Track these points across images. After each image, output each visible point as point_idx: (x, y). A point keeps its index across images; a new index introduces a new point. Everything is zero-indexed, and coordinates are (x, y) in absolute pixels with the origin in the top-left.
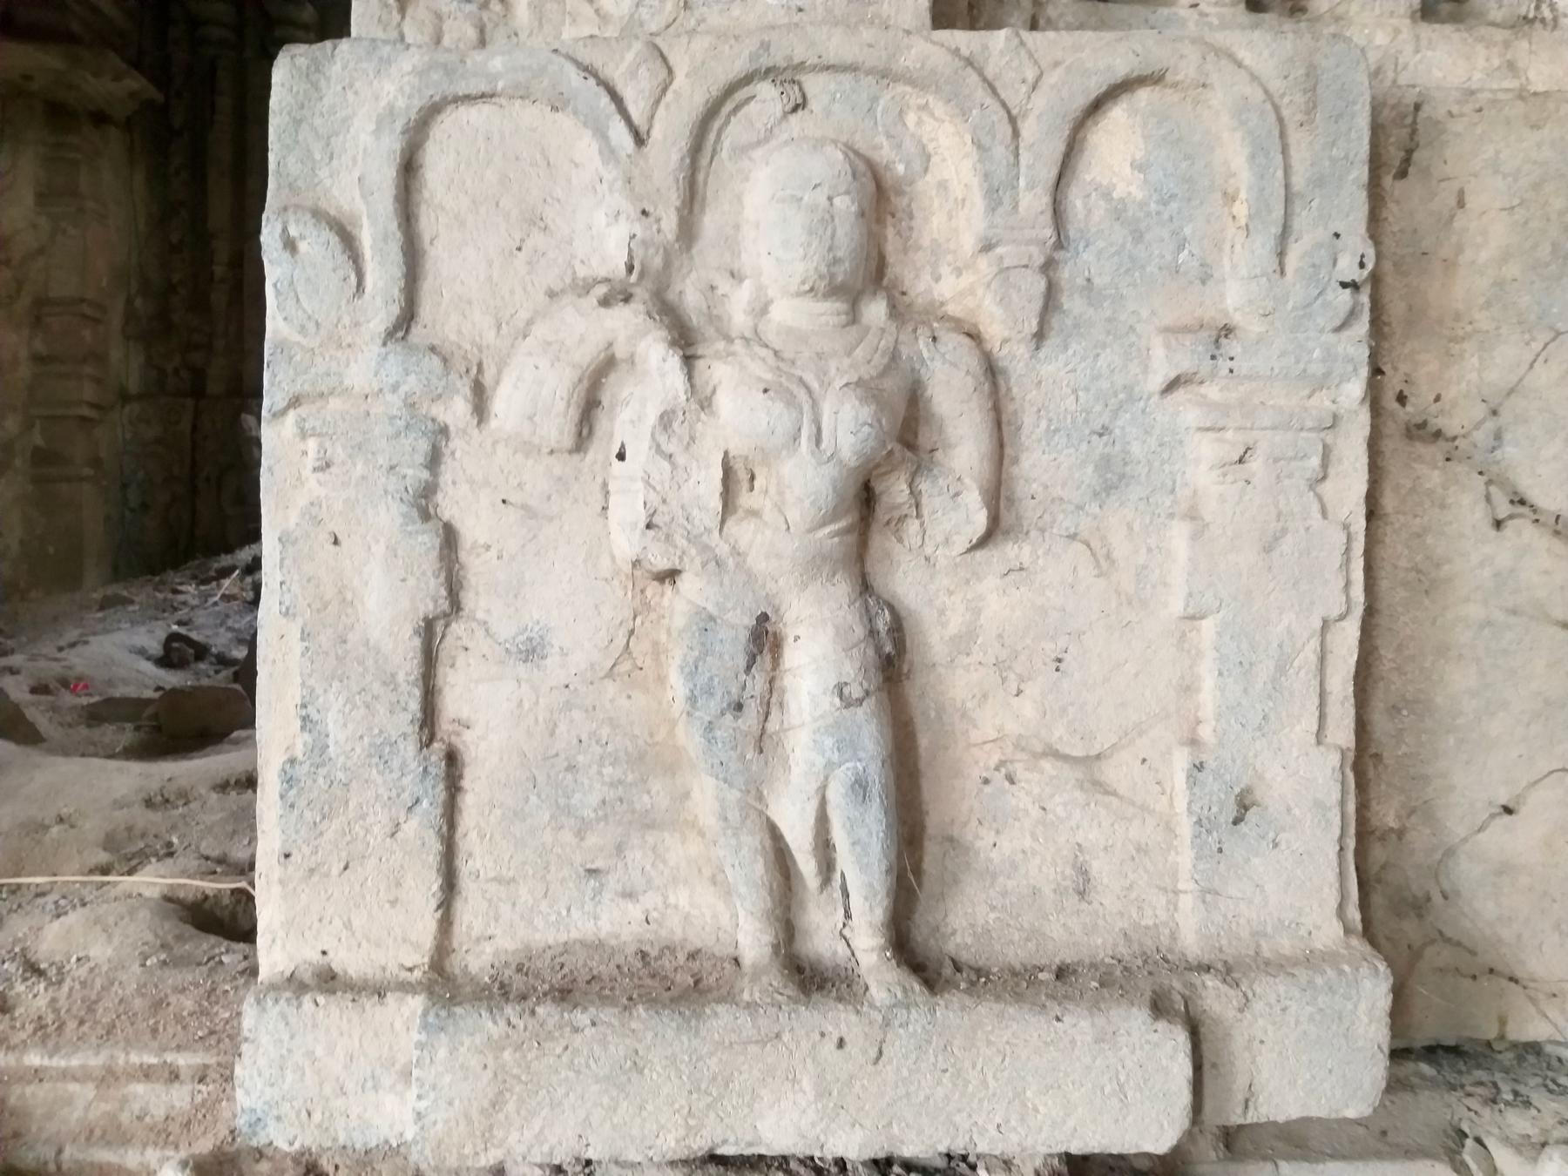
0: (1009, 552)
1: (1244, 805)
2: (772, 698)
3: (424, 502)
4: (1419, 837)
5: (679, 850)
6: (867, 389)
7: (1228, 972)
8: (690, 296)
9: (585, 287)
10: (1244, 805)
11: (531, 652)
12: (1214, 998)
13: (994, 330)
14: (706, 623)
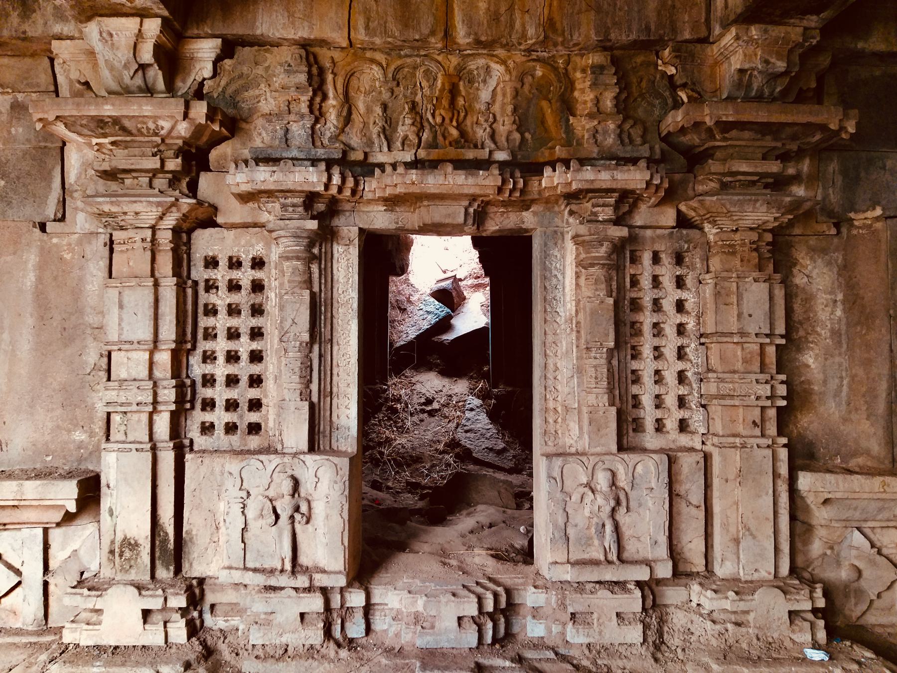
0: (629, 514)
1: (656, 543)
2: (604, 532)
3: (565, 510)
4: (679, 545)
5: (593, 548)
6: (614, 499)
7: (654, 561)
8: (593, 486)
9: (581, 485)
10: (656, 543)
11: (576, 526)
12: (653, 564)
13: (626, 489)
14: (597, 524)
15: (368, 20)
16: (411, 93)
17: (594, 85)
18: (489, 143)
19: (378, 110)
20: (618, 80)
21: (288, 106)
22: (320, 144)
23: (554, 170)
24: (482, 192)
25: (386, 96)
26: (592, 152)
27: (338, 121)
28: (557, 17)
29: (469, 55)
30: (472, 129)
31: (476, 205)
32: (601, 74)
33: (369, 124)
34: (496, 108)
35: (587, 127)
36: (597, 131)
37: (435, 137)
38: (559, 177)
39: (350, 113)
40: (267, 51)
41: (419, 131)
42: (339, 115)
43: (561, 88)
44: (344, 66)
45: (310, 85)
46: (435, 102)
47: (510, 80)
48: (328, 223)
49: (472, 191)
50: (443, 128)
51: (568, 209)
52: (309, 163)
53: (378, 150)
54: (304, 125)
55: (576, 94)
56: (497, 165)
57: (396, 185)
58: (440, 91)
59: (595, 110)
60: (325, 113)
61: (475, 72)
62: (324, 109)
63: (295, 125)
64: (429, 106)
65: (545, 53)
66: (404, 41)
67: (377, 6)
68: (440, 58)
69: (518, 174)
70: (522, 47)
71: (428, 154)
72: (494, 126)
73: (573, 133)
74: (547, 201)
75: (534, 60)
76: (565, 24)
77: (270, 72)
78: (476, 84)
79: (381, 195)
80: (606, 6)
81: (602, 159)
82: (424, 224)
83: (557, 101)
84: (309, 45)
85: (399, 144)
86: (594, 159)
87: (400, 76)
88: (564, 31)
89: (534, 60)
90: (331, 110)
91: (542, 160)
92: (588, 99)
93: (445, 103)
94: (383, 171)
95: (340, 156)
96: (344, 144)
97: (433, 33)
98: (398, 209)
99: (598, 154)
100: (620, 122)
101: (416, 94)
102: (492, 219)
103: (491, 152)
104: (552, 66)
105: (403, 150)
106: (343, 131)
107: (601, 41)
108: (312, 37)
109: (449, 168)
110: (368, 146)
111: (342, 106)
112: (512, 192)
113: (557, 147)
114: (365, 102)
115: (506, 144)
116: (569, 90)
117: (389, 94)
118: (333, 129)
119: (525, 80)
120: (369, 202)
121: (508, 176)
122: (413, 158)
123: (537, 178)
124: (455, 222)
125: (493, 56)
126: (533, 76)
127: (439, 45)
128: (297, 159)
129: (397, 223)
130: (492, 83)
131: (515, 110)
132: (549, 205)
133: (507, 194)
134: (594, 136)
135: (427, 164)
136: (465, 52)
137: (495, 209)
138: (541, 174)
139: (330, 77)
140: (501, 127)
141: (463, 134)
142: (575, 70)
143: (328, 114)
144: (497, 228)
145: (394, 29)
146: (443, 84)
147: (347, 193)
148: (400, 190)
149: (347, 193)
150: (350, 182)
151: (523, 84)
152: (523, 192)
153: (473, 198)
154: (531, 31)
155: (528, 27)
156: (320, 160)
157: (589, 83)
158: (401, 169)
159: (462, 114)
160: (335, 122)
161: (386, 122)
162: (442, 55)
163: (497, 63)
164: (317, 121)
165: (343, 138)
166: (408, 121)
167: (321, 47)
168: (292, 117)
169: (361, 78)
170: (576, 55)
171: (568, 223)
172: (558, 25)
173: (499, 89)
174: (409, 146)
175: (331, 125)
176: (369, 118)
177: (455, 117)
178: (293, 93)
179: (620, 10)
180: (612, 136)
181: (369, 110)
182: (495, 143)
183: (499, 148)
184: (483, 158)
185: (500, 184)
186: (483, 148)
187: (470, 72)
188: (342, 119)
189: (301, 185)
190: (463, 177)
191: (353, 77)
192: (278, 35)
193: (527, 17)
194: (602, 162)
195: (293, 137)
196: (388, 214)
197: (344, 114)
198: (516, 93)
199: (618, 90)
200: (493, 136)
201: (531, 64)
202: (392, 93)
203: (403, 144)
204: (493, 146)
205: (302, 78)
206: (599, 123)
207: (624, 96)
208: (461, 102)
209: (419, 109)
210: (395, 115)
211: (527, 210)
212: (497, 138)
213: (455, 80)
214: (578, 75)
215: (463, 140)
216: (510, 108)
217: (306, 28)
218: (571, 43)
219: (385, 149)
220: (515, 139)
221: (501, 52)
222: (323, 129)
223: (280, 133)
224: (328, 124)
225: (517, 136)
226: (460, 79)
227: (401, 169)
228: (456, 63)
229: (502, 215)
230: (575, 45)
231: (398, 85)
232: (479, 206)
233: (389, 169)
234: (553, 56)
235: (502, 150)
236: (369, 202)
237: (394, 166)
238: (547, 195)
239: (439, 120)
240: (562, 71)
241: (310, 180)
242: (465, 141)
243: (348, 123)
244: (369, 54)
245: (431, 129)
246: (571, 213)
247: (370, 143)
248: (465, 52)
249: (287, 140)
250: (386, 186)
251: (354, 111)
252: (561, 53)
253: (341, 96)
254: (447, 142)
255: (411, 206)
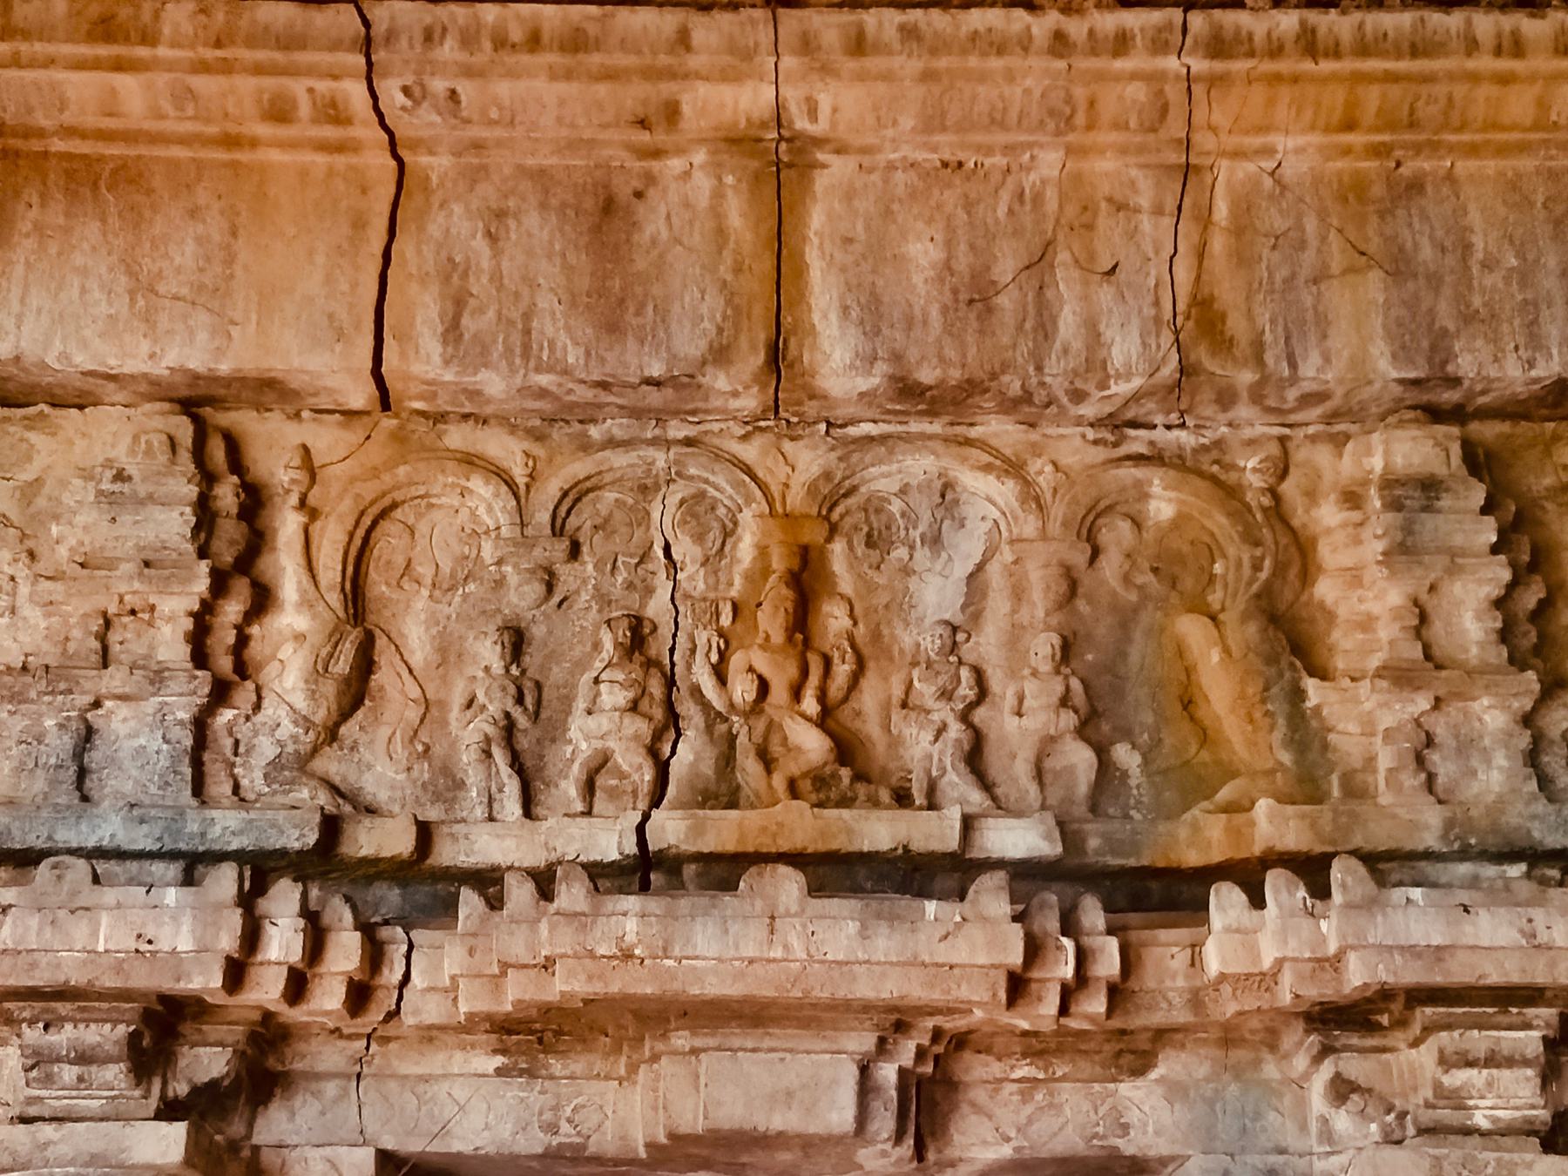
15: (458, 304)
16: (630, 586)
17: (1403, 551)
18: (960, 791)
19: (488, 653)
20: (1501, 533)
21: (102, 638)
22: (227, 789)
23: (1257, 901)
24: (936, 996)
25: (521, 596)
26: (1415, 826)
27: (312, 695)
28: (1228, 291)
29: (870, 439)
30: (887, 728)
31: (906, 1052)
32: (1426, 509)
33: (443, 705)
34: (987, 645)
35: (1386, 720)
36: (1430, 742)
37: (727, 760)
38: (1283, 934)
39: (365, 663)
40: (31, 423)
41: (658, 736)
42: (319, 669)
43: (1257, 567)
44: (353, 480)
45: (203, 553)
46: (726, 620)
47: (1044, 536)
48: (237, 1128)
49: (890, 988)
50: (760, 725)
51: (1327, 1070)
52: (174, 870)
53: (480, 812)
54: (162, 713)
55: (1325, 589)
56: (1000, 877)
57: (548, 965)
58: (748, 577)
59: (1417, 652)
60: (259, 667)
61: (896, 507)
62: (255, 650)
63: (124, 710)
64: (702, 637)
65: (1182, 435)
66: (603, 385)
67: (497, 254)
68: (749, 452)
69: (1093, 915)
70: (1089, 410)
71: (697, 830)
72: (979, 715)
73: (1325, 746)
74: (1229, 1037)
75: (1138, 459)
76: (1264, 318)
77: (41, 502)
78: (901, 553)
79: (483, 1005)
80: (1427, 252)
81: (1464, 855)
82: (673, 1136)
83: (1245, 618)
84: (211, 401)
85: (570, 789)
86: (1428, 855)
87: (582, 520)
88: (1258, 347)
89: (1138, 459)
90: (286, 652)
91: (1192, 858)
92: (1375, 608)
93: (771, 621)
94: (495, 903)
95: (312, 838)
96: (335, 790)
97: (720, 354)
98: (556, 1065)
99: (1444, 837)
100: (1528, 704)
101: (649, 591)
102: (977, 1108)
103: (968, 824)
104: (1214, 479)
105: (588, 813)
106: (332, 734)
107: (1416, 382)
108: (224, 368)
109: (789, 884)
110: (437, 797)
111: (335, 638)
112: (1068, 996)
113: (1263, 806)
114: (432, 620)
115: (1033, 789)
116: (1293, 572)
117: (536, 589)
118: (287, 728)
119: (1105, 537)
120: (430, 1035)
121: (1052, 923)
122: (631, 848)
123: (1183, 934)
124: (814, 1128)
125: (968, 442)
126: (1137, 524)
127: (749, 402)
128: (120, 855)
129: (552, 1129)
130: (967, 548)
131: (1067, 651)
132: (1240, 1055)
133: (1051, 1005)
134: (1420, 760)
135: (689, 870)
136: (853, 431)
137: (996, 1068)
138: (1197, 910)
139: (287, 525)
140: (1011, 723)
141: (846, 749)
142: (1312, 496)
143: (271, 670)
144: (1006, 1151)
145: (563, 338)
146: (762, 551)
147: (329, 997)
148: (565, 985)
149: (329, 997)
150: (345, 952)
151: (1096, 553)
152: (1117, 994)
153: (898, 1020)
154: (1124, 347)
155: (1109, 332)
156: (218, 857)
157: (1380, 546)
158: (572, 894)
159: (842, 671)
160: (301, 702)
161: (520, 700)
162: (758, 441)
163: (987, 468)
164: (221, 693)
165: (330, 764)
166: (614, 696)
167: (262, 408)
168: (114, 679)
169: (422, 528)
170: (1313, 439)
171: (1327, 1134)
172: (1236, 325)
173: (994, 570)
174: (613, 794)
175: (283, 713)
176: (445, 681)
177: (814, 680)
178: (127, 585)
179: (1488, 265)
180: (1500, 759)
181: (448, 653)
182: (986, 785)
183: (1001, 807)
184: (936, 846)
185: (1016, 958)
186: (932, 805)
187: (875, 506)
188: (329, 689)
189: (118, 968)
190: (852, 927)
191: (384, 525)
192: (83, 361)
193: (1105, 295)
194: (1464, 869)
195: (112, 761)
196: (514, 1090)
197: (342, 666)
198: (1071, 587)
199: (1506, 575)
200: (974, 758)
201: (1129, 473)
202: (550, 588)
203: (589, 788)
204: (976, 798)
205: (174, 524)
206: (1438, 703)
207: (1531, 597)
208: (834, 620)
209: (658, 647)
210: (557, 674)
211: (1139, 1071)
212: (995, 768)
213: (813, 534)
214: (1329, 515)
215: (845, 773)
216: (1044, 646)
217: (202, 336)
218: (1292, 395)
219: (511, 806)
220: (1070, 770)
221: (999, 429)
222: (243, 731)
223: (60, 744)
224: (270, 709)
225: (1080, 758)
226: (833, 530)
227: (572, 894)
228: (815, 470)
229: (1026, 1096)
230: (1308, 400)
231: (575, 552)
232: (921, 1054)
233: (520, 893)
234: (1219, 444)
235: (1018, 814)
236: (430, 1035)
237: (544, 882)
238: (1231, 1009)
239: (742, 690)
240: (1256, 499)
241: (164, 945)
242: (859, 777)
243: (357, 703)
244: (457, 437)
245: (709, 728)
246: (1342, 1089)
247: (448, 785)
248: (853, 431)
249: (82, 773)
250: (505, 966)
251: (384, 654)
252: (1248, 433)
253: (334, 599)
254: (779, 781)
255: (617, 1049)
